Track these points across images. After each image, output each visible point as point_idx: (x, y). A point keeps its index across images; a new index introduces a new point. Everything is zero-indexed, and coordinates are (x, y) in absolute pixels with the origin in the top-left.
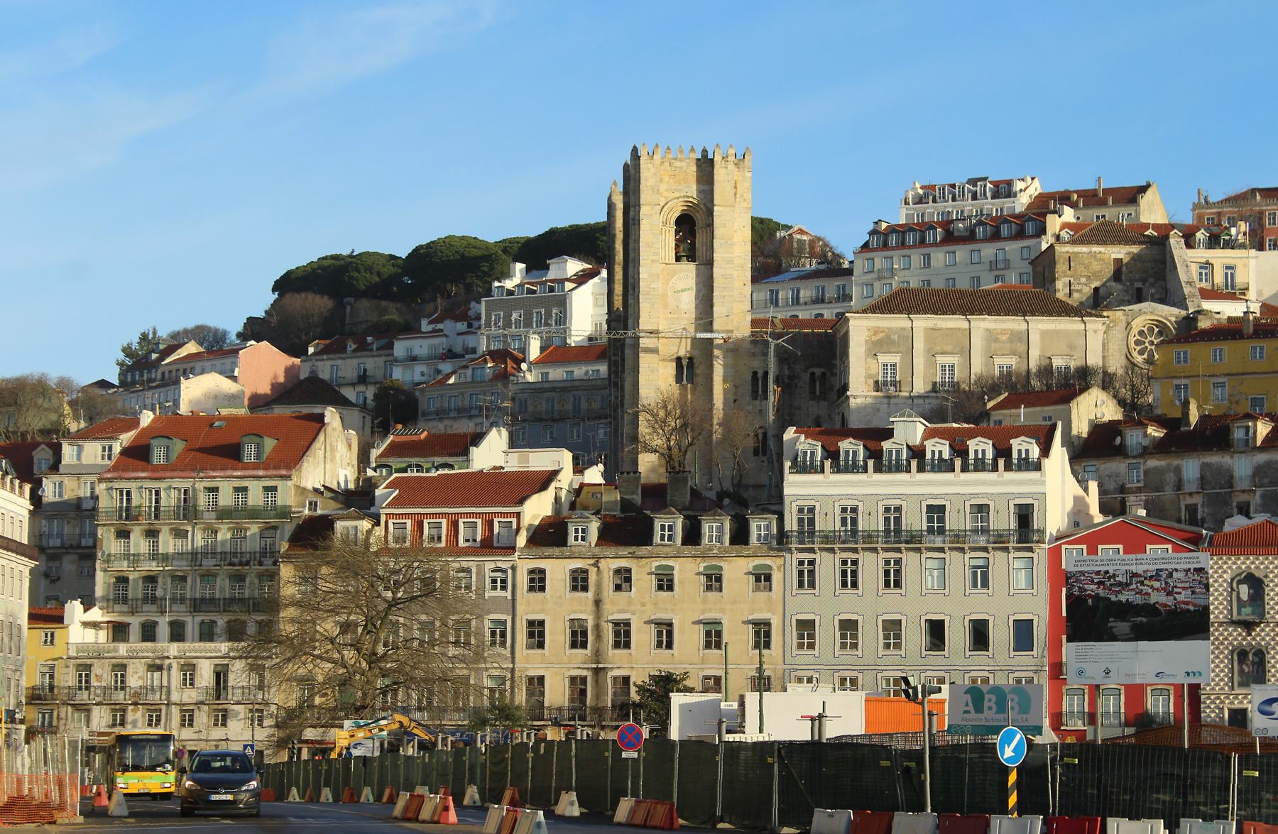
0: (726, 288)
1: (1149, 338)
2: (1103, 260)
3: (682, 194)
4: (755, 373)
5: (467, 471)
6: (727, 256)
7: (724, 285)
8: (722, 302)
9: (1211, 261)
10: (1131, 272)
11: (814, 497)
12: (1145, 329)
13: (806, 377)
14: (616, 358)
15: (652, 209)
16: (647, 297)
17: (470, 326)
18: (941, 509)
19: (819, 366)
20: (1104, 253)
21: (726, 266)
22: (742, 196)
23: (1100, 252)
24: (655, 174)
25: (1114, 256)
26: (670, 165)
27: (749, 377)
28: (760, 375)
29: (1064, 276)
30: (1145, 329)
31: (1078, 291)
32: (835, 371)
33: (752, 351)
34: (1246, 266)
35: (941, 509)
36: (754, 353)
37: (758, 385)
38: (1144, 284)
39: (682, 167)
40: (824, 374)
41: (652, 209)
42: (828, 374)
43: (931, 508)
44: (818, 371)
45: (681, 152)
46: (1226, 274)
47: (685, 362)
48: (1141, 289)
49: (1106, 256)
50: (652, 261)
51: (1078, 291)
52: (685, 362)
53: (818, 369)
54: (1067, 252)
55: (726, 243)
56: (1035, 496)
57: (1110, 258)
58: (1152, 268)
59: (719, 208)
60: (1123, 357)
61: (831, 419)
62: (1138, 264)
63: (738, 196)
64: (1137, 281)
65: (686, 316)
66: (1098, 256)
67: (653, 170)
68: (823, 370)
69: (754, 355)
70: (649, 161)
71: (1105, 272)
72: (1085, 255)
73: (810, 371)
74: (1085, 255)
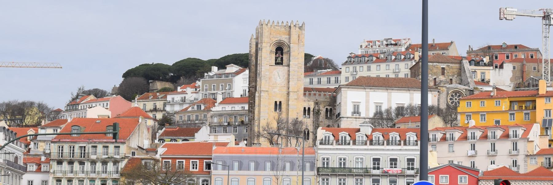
0: (294, 75)
1: (454, 99)
2: (438, 68)
3: (278, 39)
4: (305, 108)
5: (194, 142)
6: (295, 63)
7: (294, 74)
9: (476, 71)
10: (448, 73)
11: (329, 154)
12: (454, 94)
13: (324, 110)
14: (252, 101)
15: (267, 44)
16: (264, 78)
17: (196, 90)
18: (378, 160)
19: (329, 106)
20: (438, 65)
21: (294, 67)
22: (301, 40)
23: (437, 65)
24: (268, 31)
25: (442, 67)
28: (307, 109)
30: (454, 94)
32: (335, 108)
33: (304, 99)
34: (489, 72)
35: (378, 160)
37: (306, 113)
38: (453, 78)
39: (278, 29)
40: (331, 109)
41: (267, 44)
42: (333, 109)
43: (375, 160)
44: (329, 108)
45: (278, 23)
46: (482, 76)
47: (278, 103)
48: (452, 79)
49: (439, 66)
50: (266, 64)
52: (278, 103)
53: (329, 107)
55: (295, 58)
56: (415, 155)
57: (440, 67)
58: (456, 71)
59: (293, 45)
60: (446, 104)
61: (333, 126)
63: (300, 40)
64: (450, 76)
67: (267, 30)
68: (331, 107)
69: (305, 101)
70: (266, 26)
71: (438, 73)
73: (327, 107)
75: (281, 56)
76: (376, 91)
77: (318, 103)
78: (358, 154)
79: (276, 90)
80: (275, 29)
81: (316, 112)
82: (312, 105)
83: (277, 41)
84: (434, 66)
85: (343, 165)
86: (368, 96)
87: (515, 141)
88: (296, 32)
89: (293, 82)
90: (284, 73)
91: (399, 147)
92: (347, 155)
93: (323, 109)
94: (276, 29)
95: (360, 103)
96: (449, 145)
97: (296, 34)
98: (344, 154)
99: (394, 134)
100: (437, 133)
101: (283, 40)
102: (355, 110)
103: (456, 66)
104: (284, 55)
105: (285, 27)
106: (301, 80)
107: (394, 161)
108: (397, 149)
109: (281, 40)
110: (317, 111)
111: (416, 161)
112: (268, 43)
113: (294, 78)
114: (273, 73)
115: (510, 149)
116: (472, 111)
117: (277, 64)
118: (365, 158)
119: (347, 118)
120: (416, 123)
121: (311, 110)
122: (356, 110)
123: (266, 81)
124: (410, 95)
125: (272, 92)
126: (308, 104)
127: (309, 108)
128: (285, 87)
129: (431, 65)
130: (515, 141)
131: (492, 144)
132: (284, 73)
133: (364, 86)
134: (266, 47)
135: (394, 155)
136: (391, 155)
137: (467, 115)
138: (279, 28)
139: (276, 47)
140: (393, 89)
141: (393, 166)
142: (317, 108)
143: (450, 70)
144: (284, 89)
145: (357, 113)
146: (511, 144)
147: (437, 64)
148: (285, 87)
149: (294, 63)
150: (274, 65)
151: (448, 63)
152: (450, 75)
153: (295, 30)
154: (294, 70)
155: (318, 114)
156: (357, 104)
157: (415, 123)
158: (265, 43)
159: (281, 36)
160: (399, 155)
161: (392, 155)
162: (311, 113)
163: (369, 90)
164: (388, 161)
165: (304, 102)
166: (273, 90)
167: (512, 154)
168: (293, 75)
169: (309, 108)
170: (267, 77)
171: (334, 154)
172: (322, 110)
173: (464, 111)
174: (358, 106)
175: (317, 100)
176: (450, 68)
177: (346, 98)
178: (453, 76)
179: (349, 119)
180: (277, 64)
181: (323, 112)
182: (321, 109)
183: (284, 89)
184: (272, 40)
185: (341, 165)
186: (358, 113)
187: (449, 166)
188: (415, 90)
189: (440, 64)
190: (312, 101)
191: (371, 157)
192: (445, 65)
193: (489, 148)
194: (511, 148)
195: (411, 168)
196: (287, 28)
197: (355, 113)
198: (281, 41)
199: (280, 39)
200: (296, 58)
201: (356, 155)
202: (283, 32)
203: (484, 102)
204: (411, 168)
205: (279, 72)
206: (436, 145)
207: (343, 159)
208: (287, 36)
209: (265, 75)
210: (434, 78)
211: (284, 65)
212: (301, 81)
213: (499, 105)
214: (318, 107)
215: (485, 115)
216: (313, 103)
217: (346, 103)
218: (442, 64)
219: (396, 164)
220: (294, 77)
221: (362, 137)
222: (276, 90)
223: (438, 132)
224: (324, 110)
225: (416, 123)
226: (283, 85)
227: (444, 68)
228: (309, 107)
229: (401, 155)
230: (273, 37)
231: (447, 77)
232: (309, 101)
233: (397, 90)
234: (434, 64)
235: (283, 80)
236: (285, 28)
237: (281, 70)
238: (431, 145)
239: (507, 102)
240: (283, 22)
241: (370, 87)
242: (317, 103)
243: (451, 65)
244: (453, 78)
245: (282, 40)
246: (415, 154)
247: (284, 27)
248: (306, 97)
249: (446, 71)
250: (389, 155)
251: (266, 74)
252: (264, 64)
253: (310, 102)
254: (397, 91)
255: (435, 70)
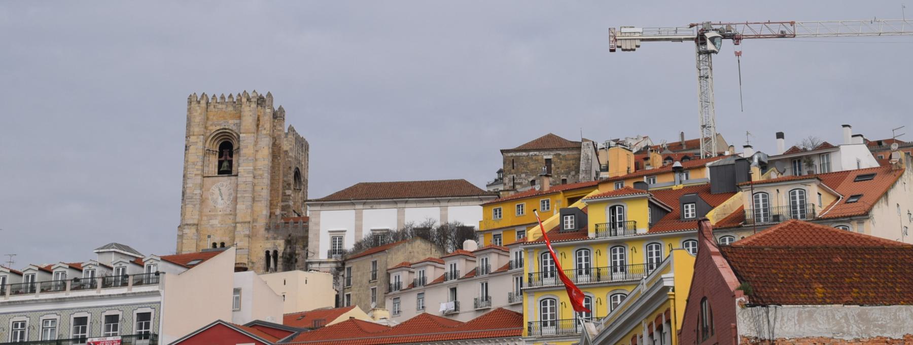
0: (245, 191)
2: (538, 160)
4: (268, 252)
7: (245, 189)
8: (243, 201)
10: (558, 168)
15: (198, 138)
20: (538, 155)
21: (246, 175)
22: (263, 126)
23: (535, 155)
24: (201, 114)
25: (545, 157)
26: (214, 107)
27: (263, 255)
29: (510, 174)
31: (519, 184)
33: (266, 236)
36: (267, 237)
38: (568, 177)
39: (222, 108)
41: (198, 138)
48: (566, 180)
49: (540, 157)
50: (196, 175)
51: (519, 184)
54: (512, 156)
55: (248, 159)
56: (153, 306)
57: (543, 158)
58: (573, 164)
59: (244, 135)
62: (563, 162)
64: (562, 174)
65: (220, 213)
66: (534, 158)
67: (199, 111)
69: (267, 239)
70: (197, 105)
72: (524, 158)
74: (524, 158)
75: (229, 158)
76: (374, 207)
77: (292, 241)
78: (48, 312)
79: (215, 222)
80: (216, 110)
81: (287, 258)
82: (280, 246)
83: (218, 130)
84: (531, 158)
85: (20, 339)
86: (359, 218)
87: (518, 274)
88: (250, 111)
89: (243, 204)
90: (230, 189)
91: (124, 290)
92: (28, 314)
93: (301, 252)
94: (218, 109)
95: (343, 233)
96: (419, 294)
97: (250, 115)
98: (22, 314)
99: (121, 261)
100: (400, 272)
101: (230, 128)
102: (336, 247)
103: (573, 154)
104: (234, 156)
105: (234, 105)
106: (261, 199)
107: (112, 320)
108: (117, 295)
109: (226, 129)
110: (288, 256)
111: (154, 318)
112: (200, 135)
113: (245, 197)
114: (211, 191)
115: (511, 291)
116: (504, 226)
117: (221, 172)
118: (60, 319)
119: (320, 263)
120: (372, 257)
121: (280, 254)
122: (337, 246)
123: (195, 205)
124: (441, 210)
125: (208, 225)
126: (274, 245)
127: (276, 252)
128: (231, 214)
129: (524, 156)
130: (518, 274)
131: (483, 284)
132: (230, 189)
133: (350, 200)
134: (197, 142)
135: (113, 308)
136: (107, 308)
137: (494, 235)
138: (224, 106)
139: (220, 143)
140: (406, 202)
141: (111, 332)
142: (288, 250)
143: (561, 163)
144: (230, 219)
145: (338, 253)
146: (513, 281)
147: (535, 153)
148: (231, 214)
149: (245, 168)
150: (217, 175)
151: (557, 149)
152: (563, 171)
153: (248, 107)
154: (246, 182)
155: (291, 262)
156: (340, 234)
157: (370, 256)
158: (194, 135)
159: (228, 122)
160: (122, 308)
161: (110, 308)
162: (280, 260)
163: (361, 207)
164: (101, 322)
165: (266, 241)
166: (209, 222)
167: (515, 303)
168: (244, 191)
169: (276, 252)
170: (196, 199)
171: (5, 315)
172: (299, 254)
173: (490, 228)
174: (341, 238)
175: (290, 236)
176: (561, 159)
177: (318, 224)
178: (568, 173)
179: (322, 265)
180: (221, 172)
181: (300, 257)
182: (297, 252)
183: (230, 219)
184: (210, 130)
185: (16, 339)
186: (341, 253)
187: (219, 323)
188: (449, 201)
189: (542, 153)
190: (281, 237)
191: (70, 315)
192: (552, 153)
193: (479, 294)
194: (514, 290)
195: (143, 333)
196: (237, 106)
197: (336, 254)
198: (227, 131)
199: (224, 127)
200: (250, 158)
201: (43, 313)
202: (230, 114)
203: (522, 207)
204: (143, 333)
205: (221, 188)
206: (399, 298)
207: (22, 324)
208: (236, 120)
209: (193, 194)
210: (530, 180)
211: (233, 174)
212: (261, 201)
213: (548, 208)
214: (290, 248)
215: (524, 231)
216: (283, 241)
217: (317, 235)
218: (546, 153)
219: (115, 328)
220: (245, 195)
221: (63, 273)
222: (215, 222)
223: (402, 270)
224: (303, 254)
225: (372, 257)
226: (228, 211)
227: (550, 159)
228: (275, 249)
229: (125, 307)
230: (211, 125)
231: (556, 176)
232: (275, 238)
233: (416, 202)
234: (531, 153)
235: (228, 203)
236: (235, 107)
237: (225, 184)
238: (393, 298)
239: (560, 201)
240: (231, 96)
241: (363, 201)
242: (288, 242)
243: (563, 153)
244: (568, 177)
245: (228, 129)
246: (152, 303)
247: (232, 105)
248: (271, 232)
249: (555, 165)
250: (104, 309)
251: (195, 193)
252: (191, 175)
253: (278, 241)
254: (415, 204)
255: (532, 166)
